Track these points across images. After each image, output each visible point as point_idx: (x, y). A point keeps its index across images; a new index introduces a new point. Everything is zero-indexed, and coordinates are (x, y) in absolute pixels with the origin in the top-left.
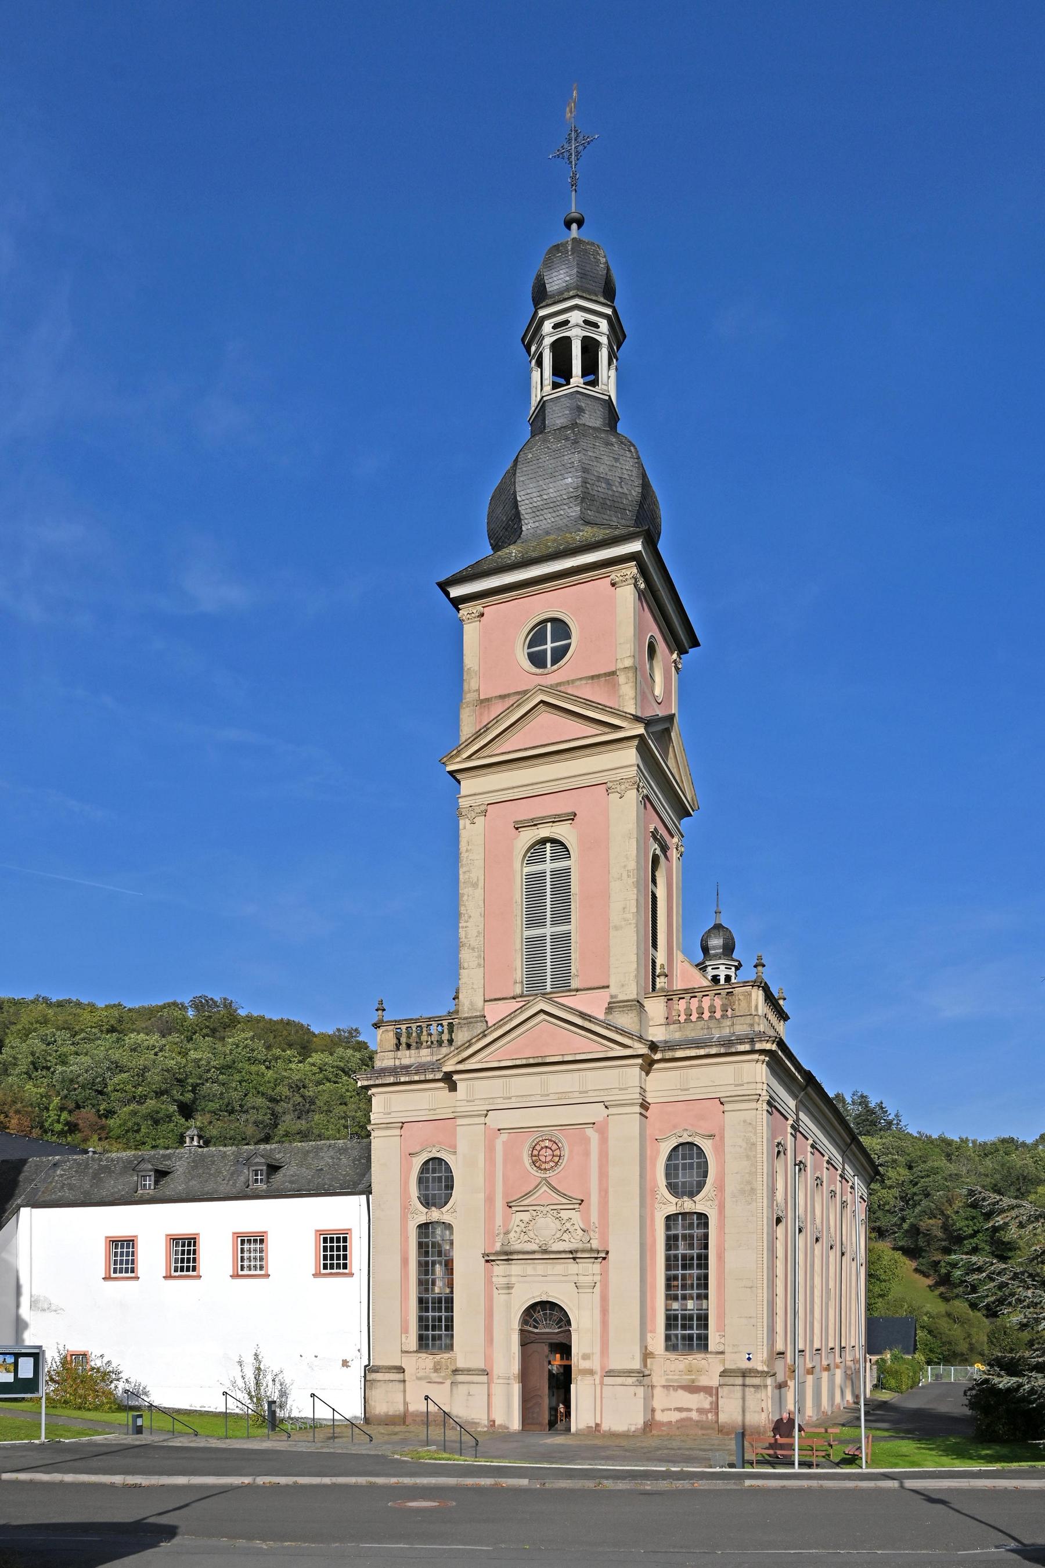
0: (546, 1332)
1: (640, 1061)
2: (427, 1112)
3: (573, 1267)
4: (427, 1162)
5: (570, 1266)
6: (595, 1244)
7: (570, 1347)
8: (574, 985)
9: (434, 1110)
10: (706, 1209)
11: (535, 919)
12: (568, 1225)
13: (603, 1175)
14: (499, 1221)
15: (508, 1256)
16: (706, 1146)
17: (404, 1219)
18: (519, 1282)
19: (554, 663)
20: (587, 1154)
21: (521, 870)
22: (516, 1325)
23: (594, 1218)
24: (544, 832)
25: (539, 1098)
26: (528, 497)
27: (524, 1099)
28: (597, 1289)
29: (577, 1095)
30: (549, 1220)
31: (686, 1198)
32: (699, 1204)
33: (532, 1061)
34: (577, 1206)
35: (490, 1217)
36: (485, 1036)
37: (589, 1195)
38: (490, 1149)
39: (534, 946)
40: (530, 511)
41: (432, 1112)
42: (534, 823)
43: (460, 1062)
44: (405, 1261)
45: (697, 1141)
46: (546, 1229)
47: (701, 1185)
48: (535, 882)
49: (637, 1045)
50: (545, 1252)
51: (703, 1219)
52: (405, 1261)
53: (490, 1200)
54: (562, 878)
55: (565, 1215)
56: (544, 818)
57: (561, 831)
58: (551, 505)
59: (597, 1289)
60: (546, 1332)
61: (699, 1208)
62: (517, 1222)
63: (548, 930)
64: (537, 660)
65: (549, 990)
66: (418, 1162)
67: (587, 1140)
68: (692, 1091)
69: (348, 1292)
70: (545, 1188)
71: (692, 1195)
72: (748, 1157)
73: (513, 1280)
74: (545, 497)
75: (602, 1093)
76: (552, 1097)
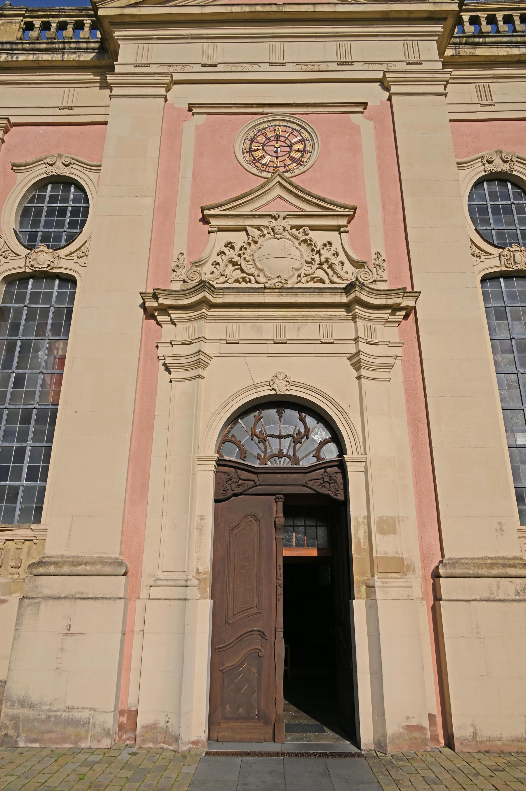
1: (436, 38)
2: (57, 111)
3: (343, 328)
4: (41, 185)
5: (336, 325)
7: (344, 505)
9: (71, 108)
12: (326, 254)
14: (180, 244)
15: (201, 299)
18: (220, 355)
20: (355, 148)
23: (377, 244)
28: (397, 374)
30: (288, 244)
34: (343, 222)
35: (162, 237)
41: (66, 112)
46: (281, 259)
53: (165, 210)
59: (397, 374)
62: (220, 246)
67: (357, 129)
68: (497, 107)
70: (278, 191)
73: (207, 348)
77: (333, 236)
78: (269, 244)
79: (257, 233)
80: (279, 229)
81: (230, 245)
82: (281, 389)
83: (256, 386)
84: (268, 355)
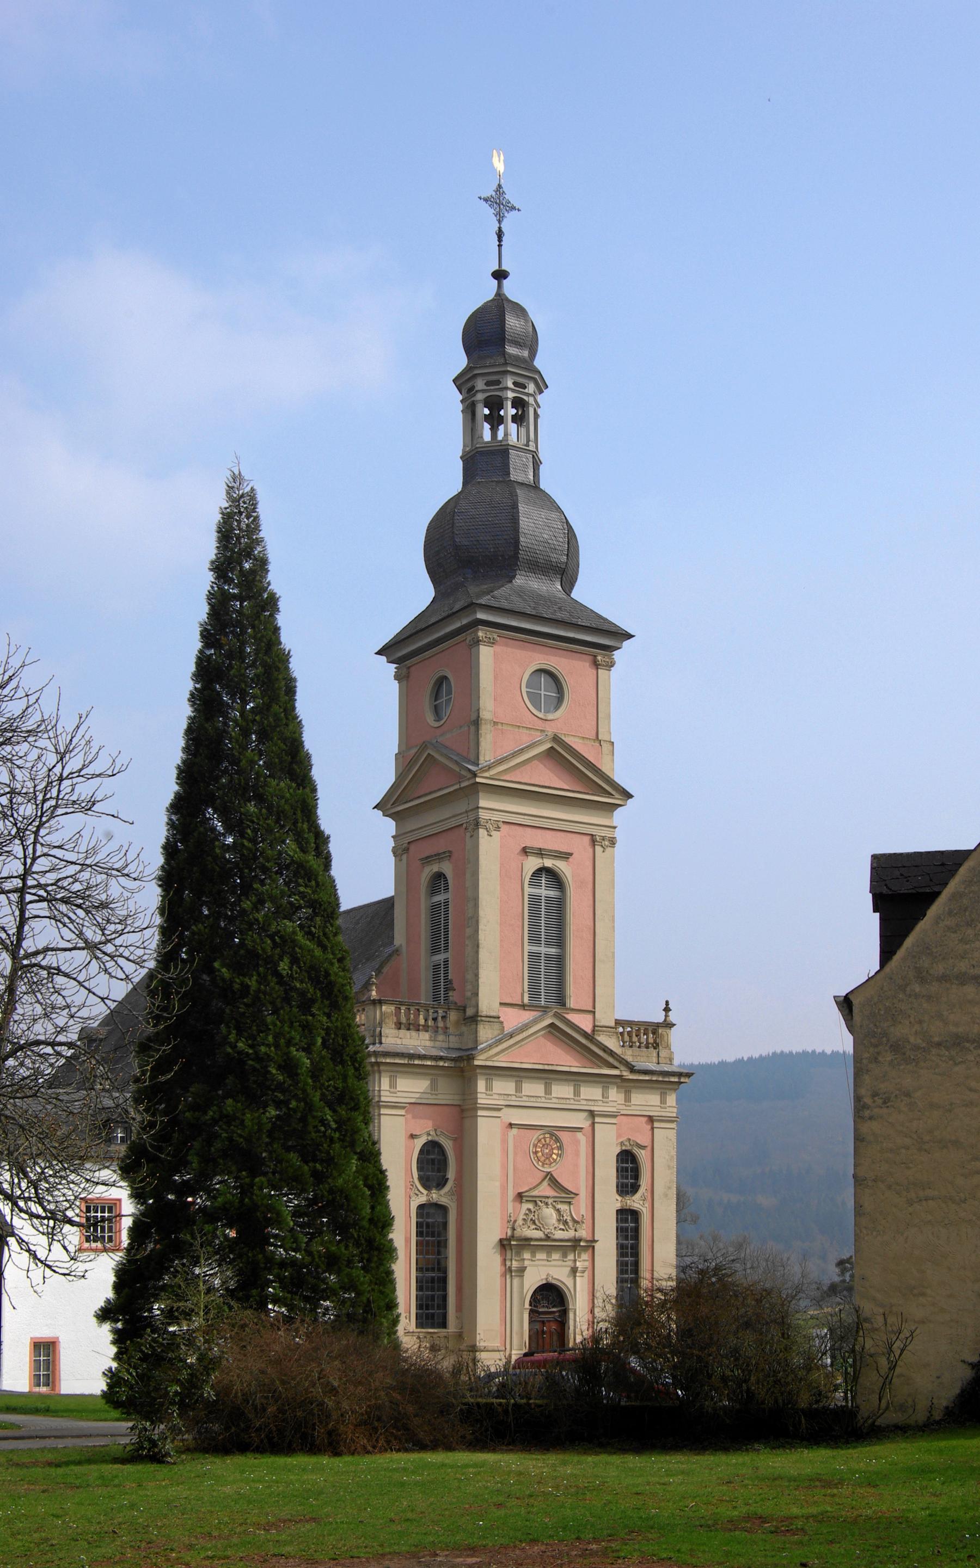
8: (568, 1005)
16: (643, 1156)
20: (577, 1154)
23: (583, 1211)
24: (548, 863)
27: (532, 1099)
29: (572, 1102)
32: (635, 1202)
33: (546, 1067)
38: (504, 1141)
42: (540, 853)
45: (636, 1150)
49: (622, 1068)
53: (504, 1188)
54: (559, 908)
56: (551, 851)
57: (561, 866)
66: (419, 1143)
67: (577, 1142)
72: (669, 1166)
73: (526, 1263)
76: (554, 1101)
81: (529, 1210)
82: (551, 1280)
84: (545, 1266)
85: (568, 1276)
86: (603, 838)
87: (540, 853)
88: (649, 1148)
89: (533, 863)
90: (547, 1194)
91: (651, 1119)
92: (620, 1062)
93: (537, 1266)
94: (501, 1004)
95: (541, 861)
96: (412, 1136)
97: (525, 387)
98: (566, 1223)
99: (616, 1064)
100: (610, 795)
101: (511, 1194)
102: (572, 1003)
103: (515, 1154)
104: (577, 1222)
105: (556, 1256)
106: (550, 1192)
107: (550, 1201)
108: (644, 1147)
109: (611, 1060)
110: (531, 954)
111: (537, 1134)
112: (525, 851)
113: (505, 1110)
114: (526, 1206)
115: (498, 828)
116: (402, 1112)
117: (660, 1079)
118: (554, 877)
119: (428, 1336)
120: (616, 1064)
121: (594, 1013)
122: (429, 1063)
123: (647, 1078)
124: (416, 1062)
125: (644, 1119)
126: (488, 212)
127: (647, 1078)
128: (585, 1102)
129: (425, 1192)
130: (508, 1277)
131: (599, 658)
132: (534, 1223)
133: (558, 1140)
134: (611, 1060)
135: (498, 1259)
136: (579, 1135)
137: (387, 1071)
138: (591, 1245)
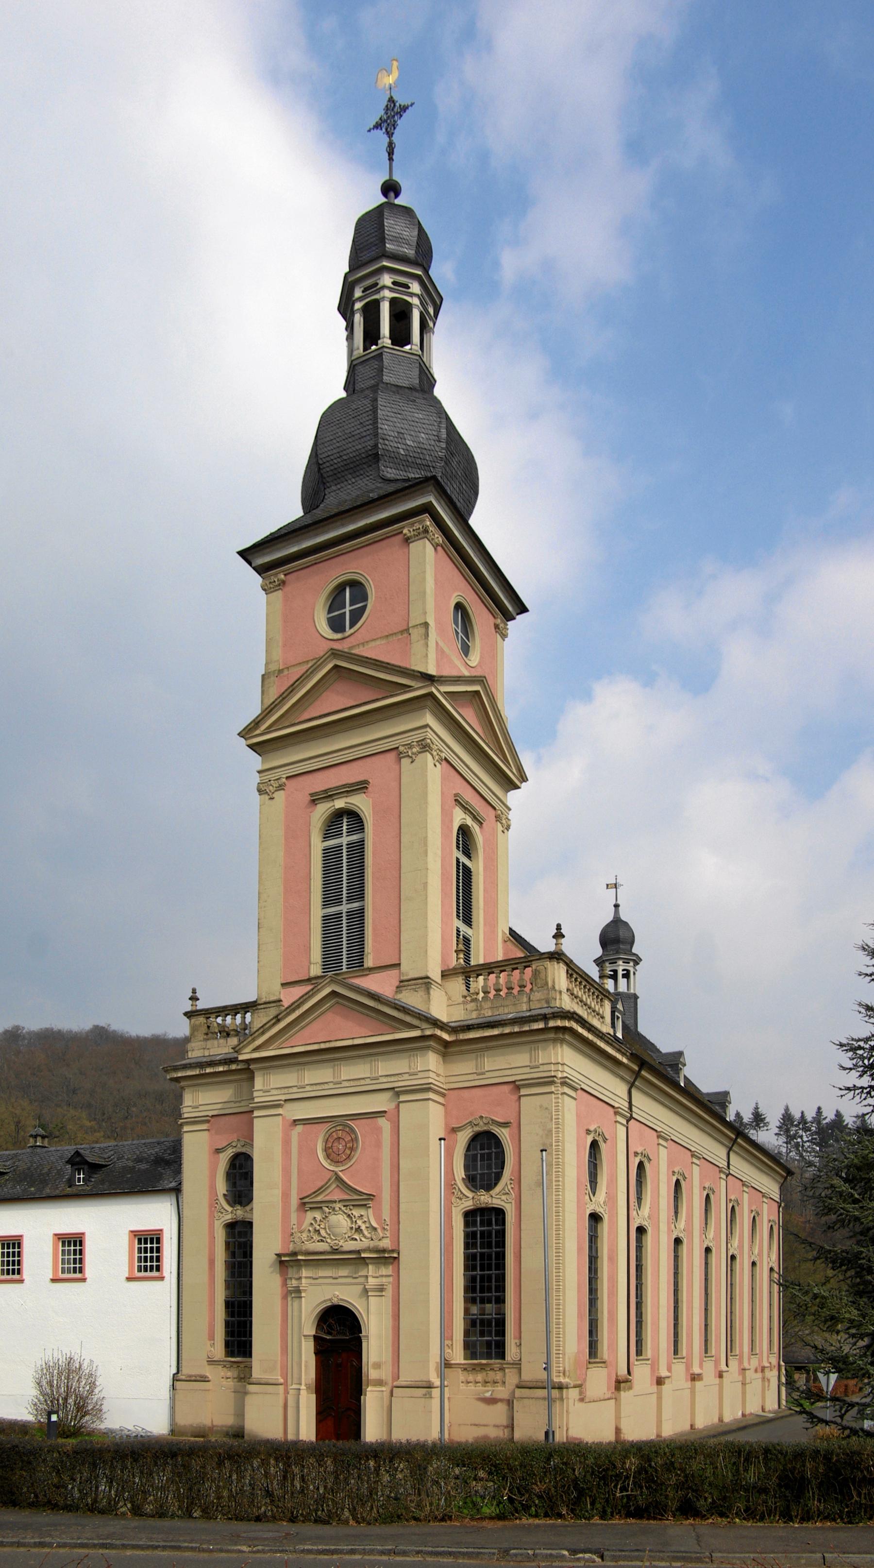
0: (339, 1337)
6: (386, 1243)
8: (366, 966)
10: (503, 1203)
11: (330, 897)
13: (396, 1167)
16: (504, 1134)
17: (212, 1218)
18: (311, 1284)
19: (351, 627)
20: (378, 1145)
21: (318, 845)
22: (310, 1329)
23: (386, 1215)
24: (340, 804)
25: (331, 1086)
26: (328, 459)
28: (389, 1292)
29: (368, 1081)
31: (483, 1192)
33: (323, 1046)
36: (279, 1021)
37: (380, 1189)
39: (330, 923)
40: (331, 473)
42: (328, 795)
43: (256, 1049)
44: (212, 1262)
45: (496, 1130)
47: (498, 1177)
48: (331, 857)
49: (424, 1025)
50: (335, 1251)
51: (500, 1213)
52: (212, 1262)
53: (286, 1195)
54: (358, 850)
55: (356, 1212)
56: (337, 788)
58: (352, 466)
60: (339, 1337)
61: (496, 1202)
63: (344, 908)
64: (336, 625)
65: (344, 970)
67: (379, 1129)
69: (160, 1294)
71: (489, 1188)
74: (345, 457)
75: (392, 1079)
77: (363, 1212)
78: (333, 1218)
79: (327, 1210)
80: (337, 1209)
82: (335, 1301)
83: (325, 1301)
85: (360, 1296)
86: (410, 746)
87: (328, 795)
88: (515, 1125)
89: (323, 810)
90: (335, 1198)
91: (516, 1086)
92: (420, 1020)
93: (320, 1284)
94: (283, 985)
95: (331, 804)
96: (218, 1151)
97: (377, 284)
98: (358, 1230)
99: (415, 1022)
100: (406, 688)
101: (294, 1202)
102: (369, 962)
103: (300, 1153)
104: (375, 1229)
105: (343, 1272)
106: (338, 1195)
107: (337, 1206)
108: (506, 1125)
109: (408, 1019)
110: (326, 918)
111: (324, 1128)
112: (315, 799)
113: (288, 1106)
114: (310, 1215)
115: (281, 787)
116: (205, 1126)
117: (516, 1029)
118: (354, 818)
119: (235, 1366)
120: (415, 1022)
121: (399, 965)
122: (221, 1069)
123: (496, 1032)
124: (208, 1070)
125: (506, 1088)
126: (380, 134)
127: (496, 1032)
128: (384, 1080)
129: (229, 1209)
130: (289, 1299)
131: (405, 531)
132: (317, 1232)
133: (352, 1130)
134: (408, 1019)
135: (277, 1279)
136: (382, 1122)
137: (189, 1086)
138: (388, 1258)
